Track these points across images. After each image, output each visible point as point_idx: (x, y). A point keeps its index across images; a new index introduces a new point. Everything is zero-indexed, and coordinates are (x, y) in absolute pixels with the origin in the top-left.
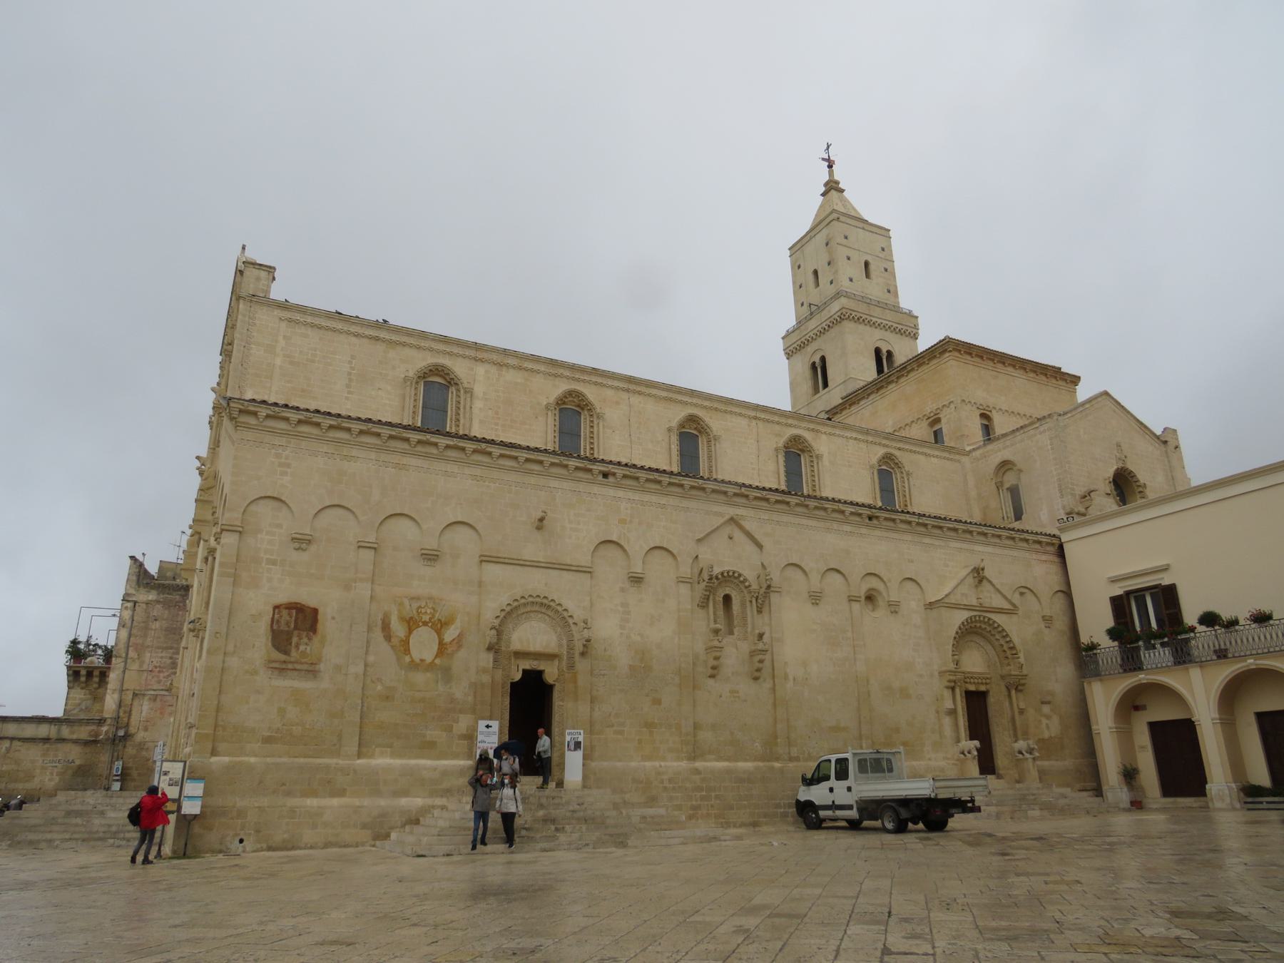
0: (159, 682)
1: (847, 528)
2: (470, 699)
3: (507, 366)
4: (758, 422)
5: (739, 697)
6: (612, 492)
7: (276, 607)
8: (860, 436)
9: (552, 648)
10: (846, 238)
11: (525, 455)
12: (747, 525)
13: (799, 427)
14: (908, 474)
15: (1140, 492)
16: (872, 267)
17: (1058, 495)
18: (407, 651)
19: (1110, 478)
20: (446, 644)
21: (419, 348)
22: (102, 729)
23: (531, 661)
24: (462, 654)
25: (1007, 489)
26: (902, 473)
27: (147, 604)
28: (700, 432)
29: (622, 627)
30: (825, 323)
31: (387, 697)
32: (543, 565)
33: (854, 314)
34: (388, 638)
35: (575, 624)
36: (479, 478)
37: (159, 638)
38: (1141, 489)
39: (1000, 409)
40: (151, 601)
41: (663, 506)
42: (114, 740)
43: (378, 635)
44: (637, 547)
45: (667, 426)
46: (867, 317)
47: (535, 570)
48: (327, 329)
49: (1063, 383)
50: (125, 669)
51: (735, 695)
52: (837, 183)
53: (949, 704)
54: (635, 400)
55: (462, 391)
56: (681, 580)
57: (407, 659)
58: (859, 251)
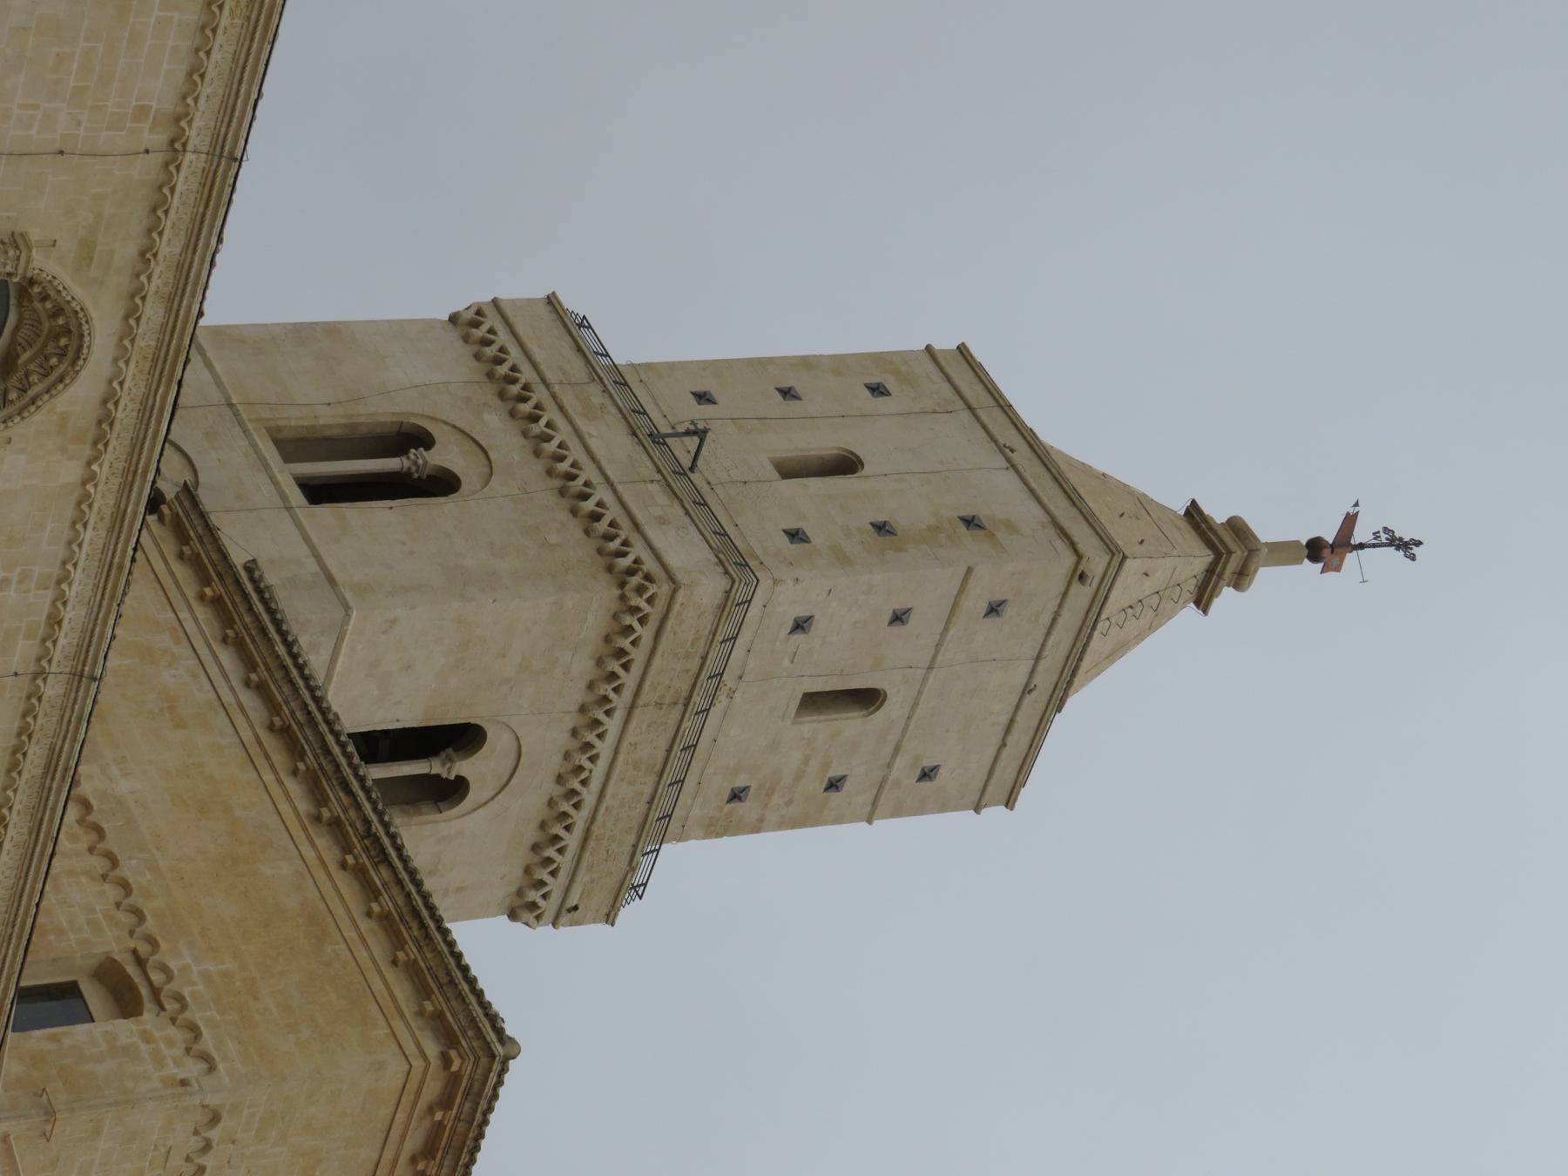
4: (157, 159)
8: (66, 639)
10: (994, 610)
13: (122, 355)
16: (851, 723)
30: (608, 498)
33: (645, 633)
46: (627, 694)
52: (1241, 579)
58: (930, 668)
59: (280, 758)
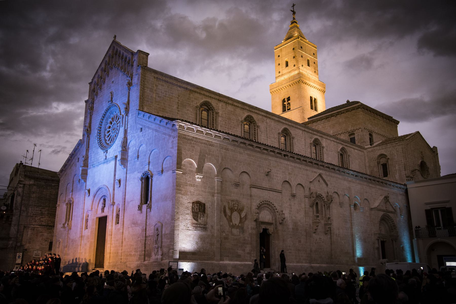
0: (35, 221)
1: (350, 179)
2: (250, 239)
3: (228, 103)
5: (321, 241)
6: (286, 162)
7: (193, 203)
9: (270, 221)
11: (263, 147)
12: (324, 177)
14: (349, 156)
15: (427, 170)
17: (404, 170)
18: (231, 221)
19: (419, 164)
20: (242, 218)
21: (200, 94)
22: (9, 242)
23: (265, 225)
24: (247, 222)
25: (381, 164)
26: (347, 155)
27: (29, 185)
28: (287, 135)
29: (290, 214)
31: (226, 238)
32: (268, 189)
34: (226, 215)
35: (277, 212)
36: (249, 155)
37: (35, 201)
38: (427, 169)
39: (375, 132)
40: (31, 184)
41: (300, 168)
42: (15, 248)
43: (223, 214)
44: (294, 183)
45: (278, 132)
47: (266, 191)
48: (170, 83)
49: (393, 123)
50: (20, 215)
51: (321, 240)
53: (377, 245)
54: (268, 120)
55: (215, 113)
56: (305, 197)
57: (231, 224)
59: (329, 119)
